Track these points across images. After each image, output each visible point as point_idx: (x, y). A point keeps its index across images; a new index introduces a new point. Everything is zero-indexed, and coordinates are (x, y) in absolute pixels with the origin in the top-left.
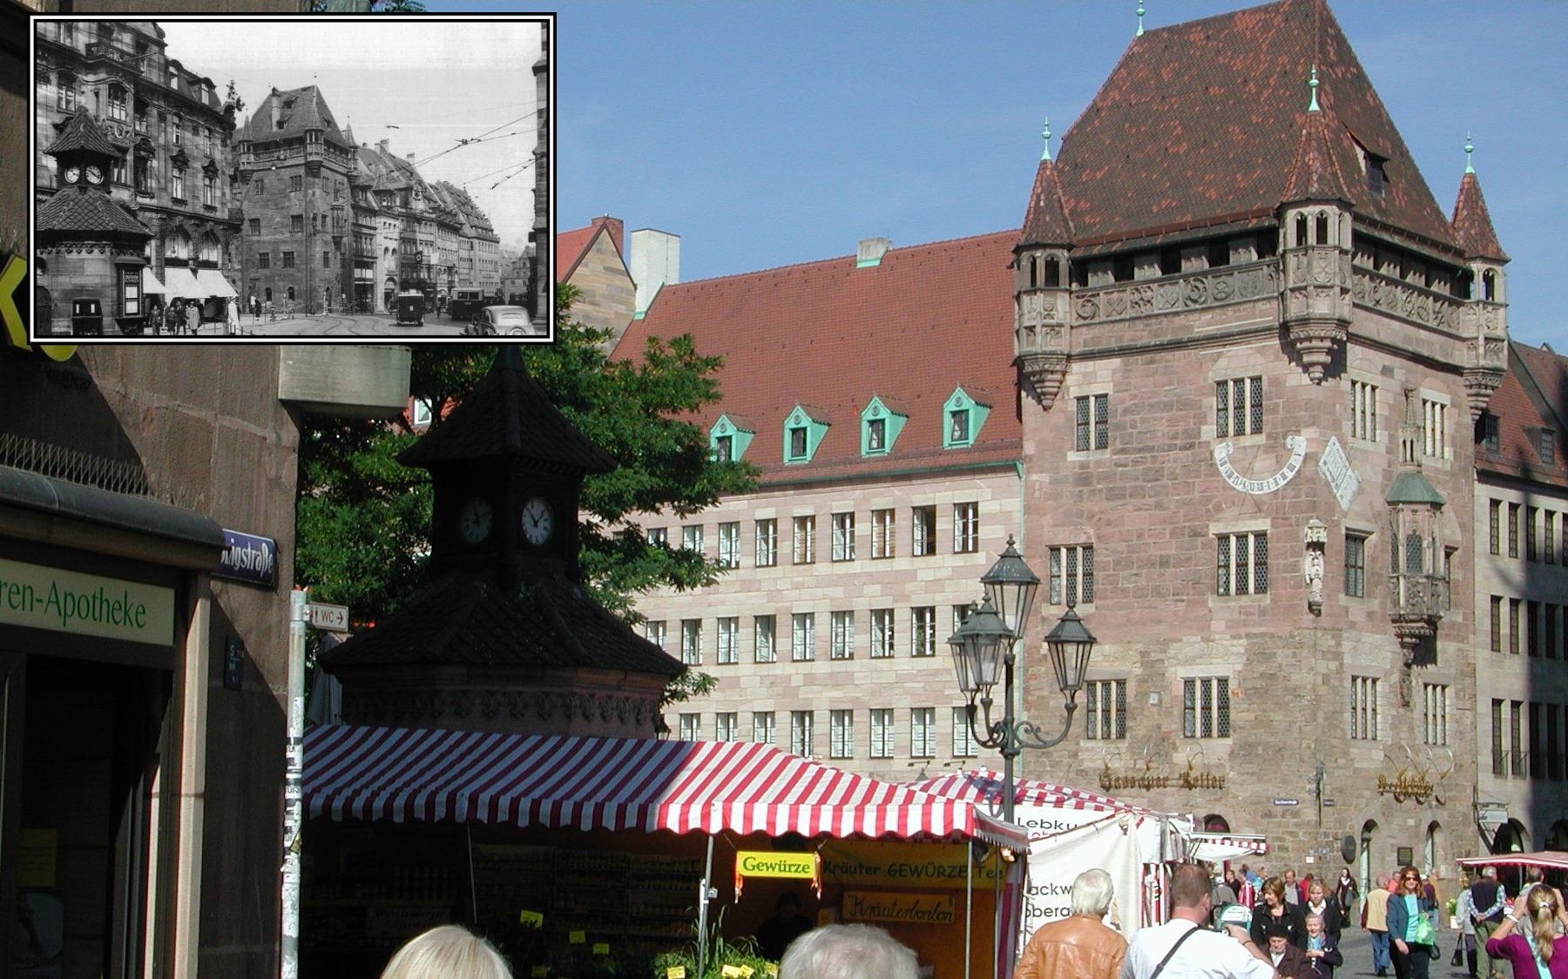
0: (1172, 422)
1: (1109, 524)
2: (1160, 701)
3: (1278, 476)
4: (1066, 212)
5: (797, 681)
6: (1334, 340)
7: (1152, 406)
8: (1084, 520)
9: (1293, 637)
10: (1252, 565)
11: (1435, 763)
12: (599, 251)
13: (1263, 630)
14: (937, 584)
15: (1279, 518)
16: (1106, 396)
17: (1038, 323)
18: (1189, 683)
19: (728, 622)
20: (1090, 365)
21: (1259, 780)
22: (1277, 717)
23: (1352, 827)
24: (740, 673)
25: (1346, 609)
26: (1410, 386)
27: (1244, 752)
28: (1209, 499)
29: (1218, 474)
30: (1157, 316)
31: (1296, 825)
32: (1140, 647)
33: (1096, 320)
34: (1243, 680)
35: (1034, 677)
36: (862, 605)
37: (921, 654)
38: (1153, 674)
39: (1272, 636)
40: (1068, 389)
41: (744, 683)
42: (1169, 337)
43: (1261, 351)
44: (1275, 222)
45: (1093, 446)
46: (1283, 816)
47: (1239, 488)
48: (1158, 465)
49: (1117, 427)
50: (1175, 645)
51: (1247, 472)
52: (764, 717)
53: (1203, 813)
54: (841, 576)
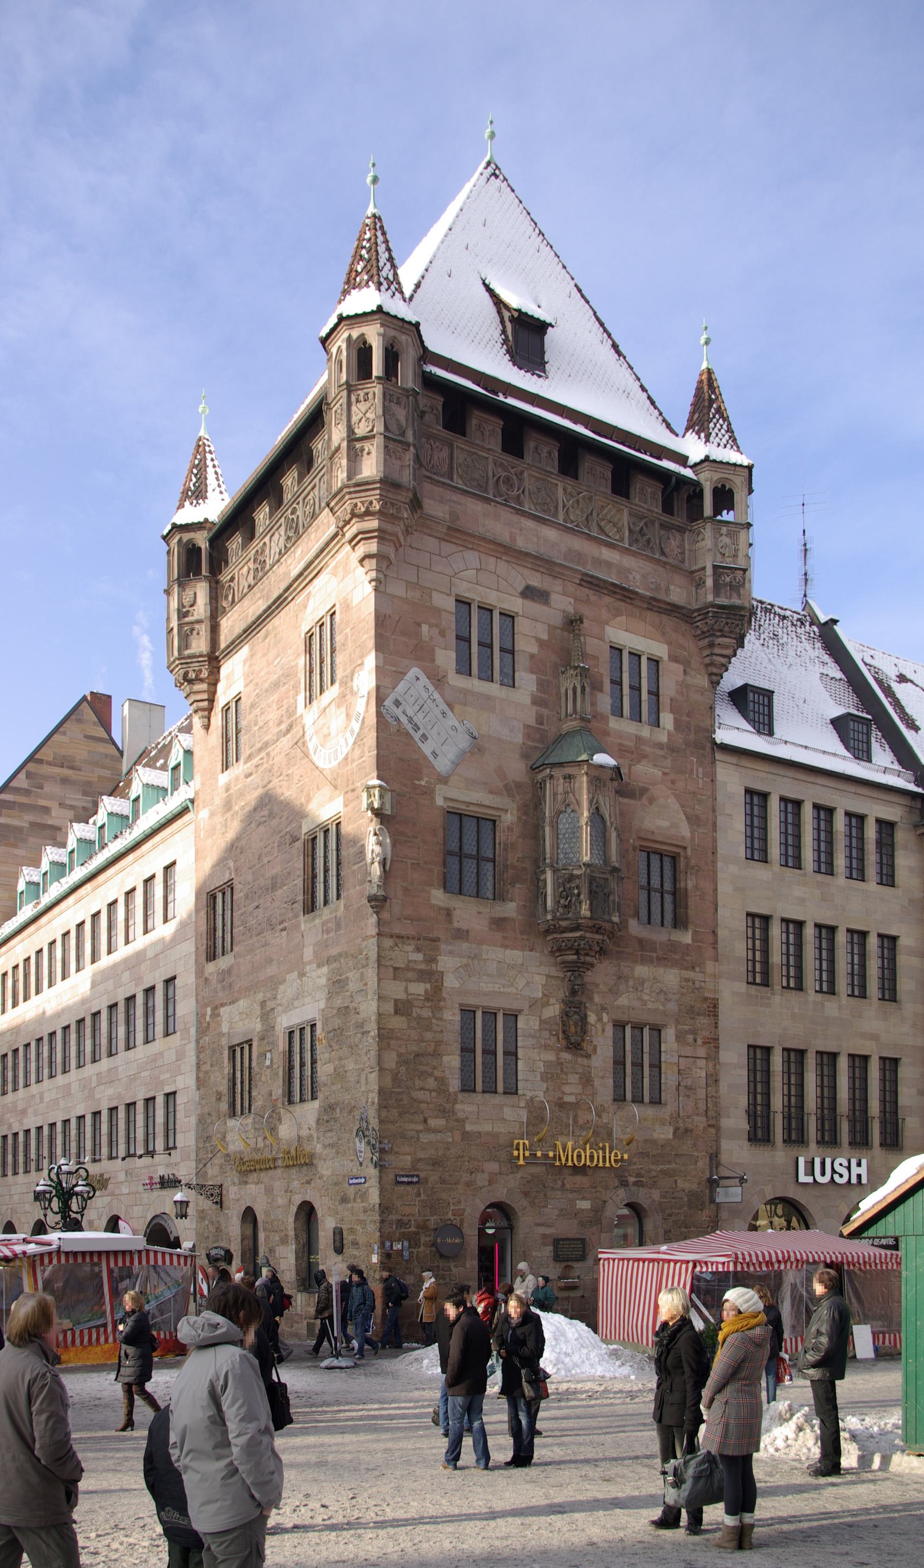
12: (79, 721)
23: (459, 1213)
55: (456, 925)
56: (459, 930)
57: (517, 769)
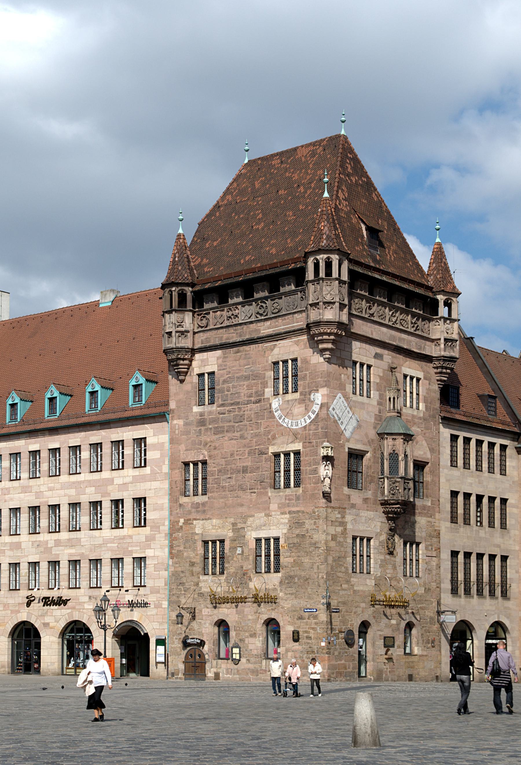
0: (249, 387)
1: (215, 449)
2: (243, 552)
4: (192, 264)
5: (51, 544)
6: (336, 334)
8: (202, 447)
9: (314, 513)
10: (289, 470)
11: (411, 588)
13: (298, 509)
14: (124, 486)
15: (307, 442)
17: (173, 330)
18: (258, 540)
19: (15, 511)
20: (205, 355)
22: (306, 560)
24: (21, 540)
25: (349, 497)
26: (395, 366)
27: (288, 581)
29: (274, 417)
30: (241, 324)
31: (316, 623)
32: (232, 520)
33: (208, 328)
34: (287, 538)
36: (85, 499)
37: (117, 527)
38: (239, 536)
39: (303, 512)
40: (193, 369)
41: (23, 546)
42: (247, 337)
43: (297, 343)
44: (304, 265)
45: (207, 403)
46: (309, 619)
47: (285, 425)
48: (242, 413)
49: (221, 391)
50: (251, 519)
52: (34, 565)
53: (265, 617)
54: (74, 483)
55: (352, 502)
56: (352, 504)
57: (372, 434)
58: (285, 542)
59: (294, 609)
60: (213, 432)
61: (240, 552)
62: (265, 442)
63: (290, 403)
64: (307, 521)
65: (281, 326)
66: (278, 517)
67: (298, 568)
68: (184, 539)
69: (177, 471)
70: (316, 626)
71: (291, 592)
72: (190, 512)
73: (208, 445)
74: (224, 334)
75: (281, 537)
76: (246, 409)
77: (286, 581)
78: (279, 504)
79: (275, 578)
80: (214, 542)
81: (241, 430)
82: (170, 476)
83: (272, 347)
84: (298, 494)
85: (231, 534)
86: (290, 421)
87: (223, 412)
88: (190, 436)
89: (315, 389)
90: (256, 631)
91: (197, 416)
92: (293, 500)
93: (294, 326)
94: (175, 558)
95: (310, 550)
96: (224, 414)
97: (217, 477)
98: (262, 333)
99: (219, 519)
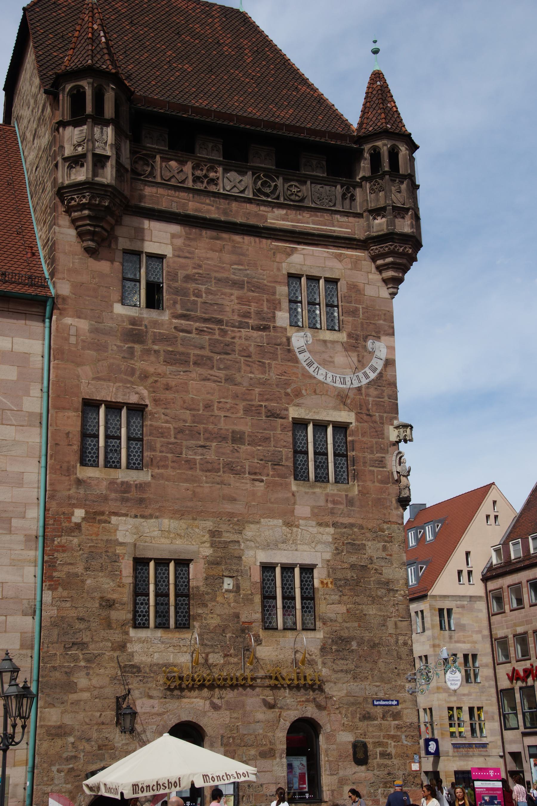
1: (168, 388)
3: (360, 374)
7: (219, 280)
9: (383, 530)
13: (351, 520)
16: (161, 258)
18: (268, 568)
21: (355, 678)
22: (372, 611)
28: (287, 384)
29: (296, 361)
32: (209, 524)
34: (332, 569)
35: (63, 548)
39: (361, 527)
40: (116, 238)
43: (339, 257)
46: (384, 718)
47: (321, 378)
48: (228, 339)
51: (326, 363)
53: (293, 715)
58: (329, 576)
59: (352, 699)
60: (162, 358)
61: (231, 587)
62: (280, 398)
63: (329, 345)
64: (369, 543)
65: (308, 223)
66: (311, 529)
67: (356, 624)
68: (87, 550)
69: (71, 414)
70: (399, 733)
71: (345, 668)
72: (105, 499)
73: (150, 380)
74: (189, 201)
75: (320, 565)
76: (238, 335)
77: (334, 647)
78: (313, 508)
79: (310, 641)
80: (162, 563)
81: (227, 368)
82: (47, 421)
83: (288, 250)
84: (350, 495)
85: (207, 551)
86: (330, 375)
87: (189, 328)
88: (106, 354)
89: (373, 334)
90: (274, 744)
91: (123, 322)
92: (341, 503)
93: (334, 231)
94: (60, 589)
95: (379, 593)
96: (189, 332)
97: (172, 440)
98: (271, 223)
99: (176, 519)
